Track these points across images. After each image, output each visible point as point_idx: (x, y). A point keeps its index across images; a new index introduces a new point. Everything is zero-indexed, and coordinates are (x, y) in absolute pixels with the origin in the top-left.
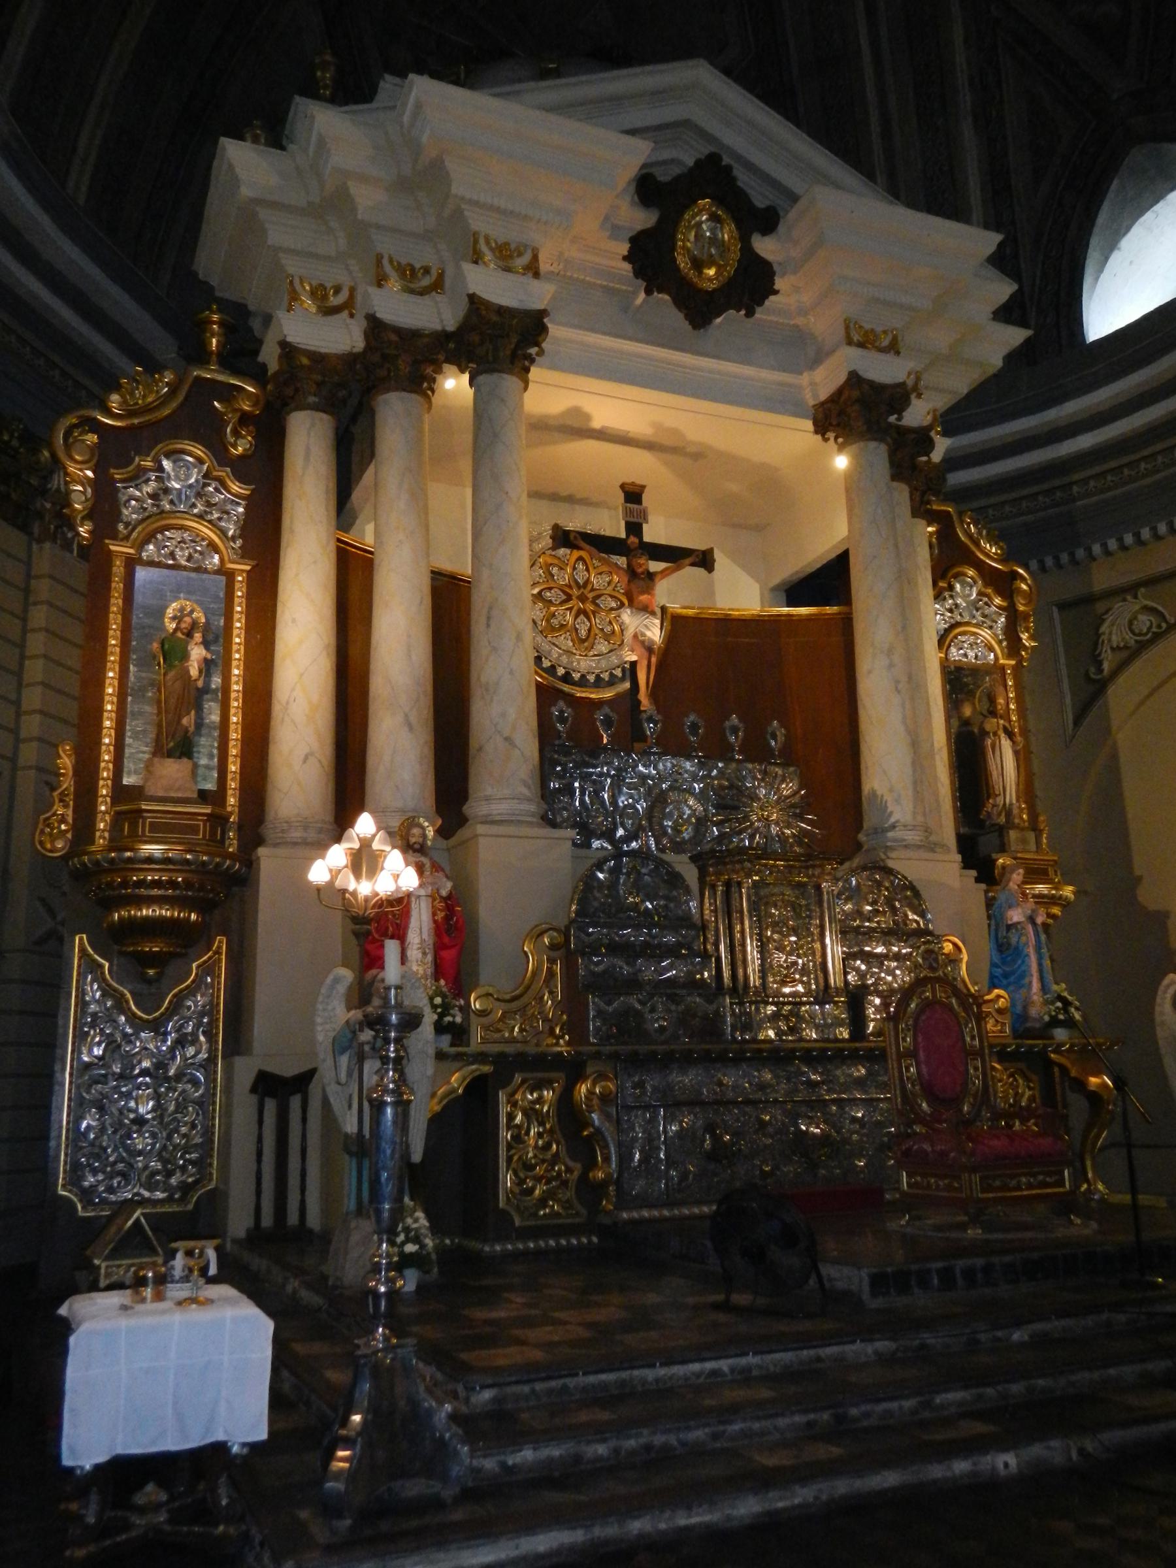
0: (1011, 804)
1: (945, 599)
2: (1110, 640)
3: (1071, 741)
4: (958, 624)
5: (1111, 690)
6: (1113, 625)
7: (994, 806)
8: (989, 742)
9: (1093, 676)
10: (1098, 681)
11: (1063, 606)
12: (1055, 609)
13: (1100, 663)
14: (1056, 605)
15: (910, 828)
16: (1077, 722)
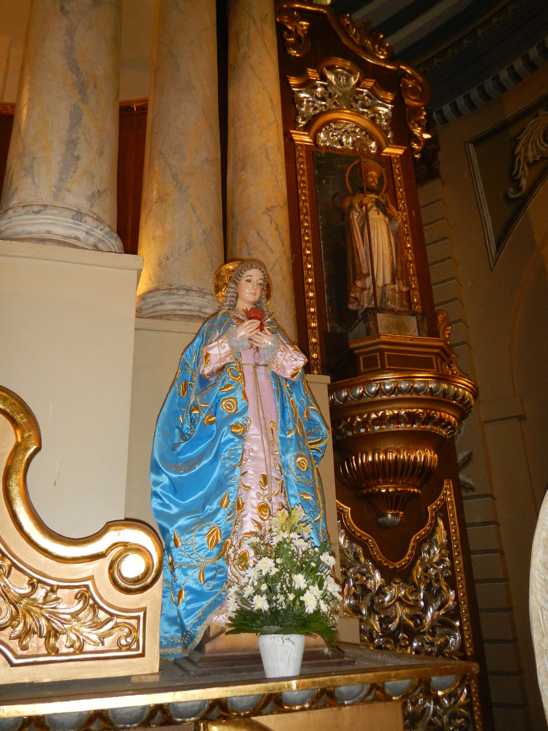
0: (385, 286)
1: (316, 87)
2: (526, 158)
3: (494, 265)
4: (330, 111)
5: (531, 205)
6: (528, 143)
7: (363, 289)
8: (355, 216)
9: (512, 196)
10: (516, 199)
11: (477, 142)
12: (471, 146)
13: (519, 181)
14: (471, 142)
15: (36, 209)
16: (500, 242)
